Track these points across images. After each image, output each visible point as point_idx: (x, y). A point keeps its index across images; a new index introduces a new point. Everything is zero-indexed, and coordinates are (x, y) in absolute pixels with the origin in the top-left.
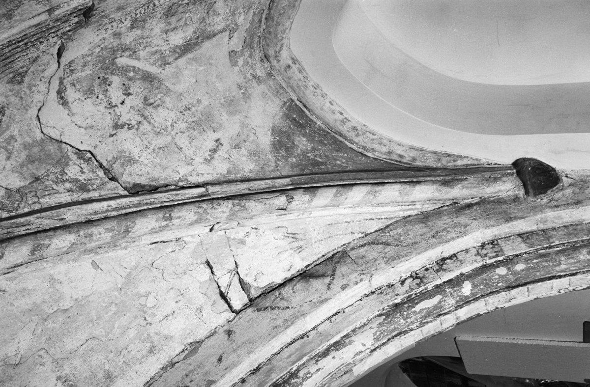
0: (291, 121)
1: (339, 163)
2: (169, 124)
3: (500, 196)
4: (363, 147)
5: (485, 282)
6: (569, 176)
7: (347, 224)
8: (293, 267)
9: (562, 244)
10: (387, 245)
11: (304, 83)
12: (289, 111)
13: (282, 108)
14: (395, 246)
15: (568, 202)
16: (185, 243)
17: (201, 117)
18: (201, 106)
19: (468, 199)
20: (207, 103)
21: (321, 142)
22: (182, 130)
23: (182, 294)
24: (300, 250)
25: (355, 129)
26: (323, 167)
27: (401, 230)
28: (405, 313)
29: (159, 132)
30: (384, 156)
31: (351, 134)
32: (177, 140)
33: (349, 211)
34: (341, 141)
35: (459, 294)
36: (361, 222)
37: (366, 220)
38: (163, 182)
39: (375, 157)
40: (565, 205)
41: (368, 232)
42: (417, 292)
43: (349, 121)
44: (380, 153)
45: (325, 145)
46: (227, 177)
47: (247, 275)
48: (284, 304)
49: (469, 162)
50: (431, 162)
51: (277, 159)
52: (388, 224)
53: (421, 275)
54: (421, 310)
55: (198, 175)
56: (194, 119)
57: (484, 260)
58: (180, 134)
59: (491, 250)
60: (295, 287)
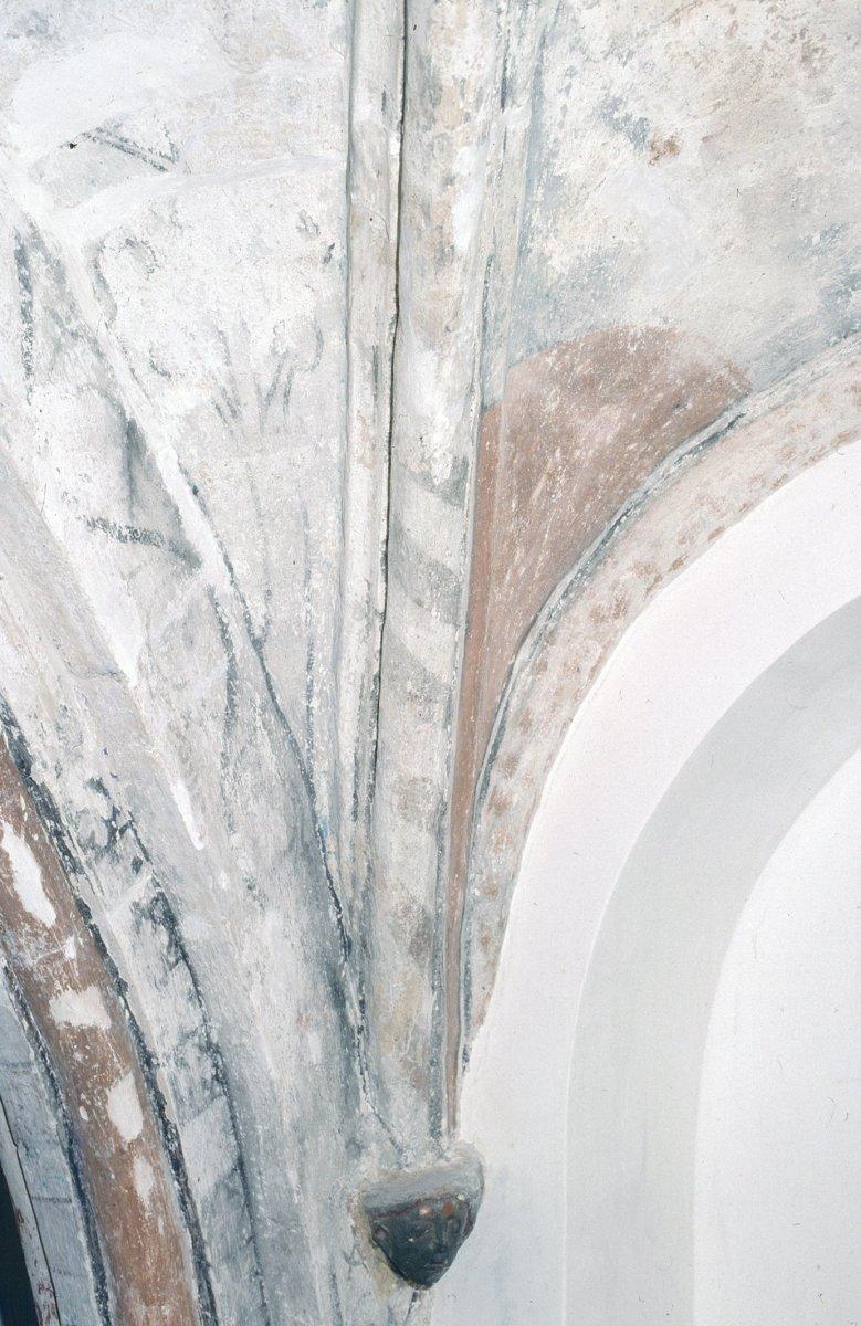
0: (678, 394)
1: (517, 558)
3: (362, 1094)
4: (552, 633)
5: (97, 1066)
6: (418, 1302)
9: (212, 1302)
10: (227, 726)
11: (801, 449)
13: (728, 365)
14: (223, 754)
15: (343, 1314)
19: (360, 990)
21: (591, 490)
22: (741, 27)
24: (227, 412)
25: (621, 609)
26: (514, 505)
27: (273, 769)
30: (514, 702)
31: (601, 593)
33: (356, 588)
34: (579, 557)
35: (57, 983)
37: (311, 646)
39: (515, 672)
40: (338, 1305)
42: (66, 839)
43: (649, 590)
44: (530, 689)
45: (579, 507)
48: (41, 360)
49: (475, 990)
50: (487, 862)
51: (565, 348)
52: (289, 717)
53: (119, 847)
55: (571, 72)
56: (766, 72)
57: (168, 1058)
58: (727, 22)
59: (197, 1079)
60: (95, 393)
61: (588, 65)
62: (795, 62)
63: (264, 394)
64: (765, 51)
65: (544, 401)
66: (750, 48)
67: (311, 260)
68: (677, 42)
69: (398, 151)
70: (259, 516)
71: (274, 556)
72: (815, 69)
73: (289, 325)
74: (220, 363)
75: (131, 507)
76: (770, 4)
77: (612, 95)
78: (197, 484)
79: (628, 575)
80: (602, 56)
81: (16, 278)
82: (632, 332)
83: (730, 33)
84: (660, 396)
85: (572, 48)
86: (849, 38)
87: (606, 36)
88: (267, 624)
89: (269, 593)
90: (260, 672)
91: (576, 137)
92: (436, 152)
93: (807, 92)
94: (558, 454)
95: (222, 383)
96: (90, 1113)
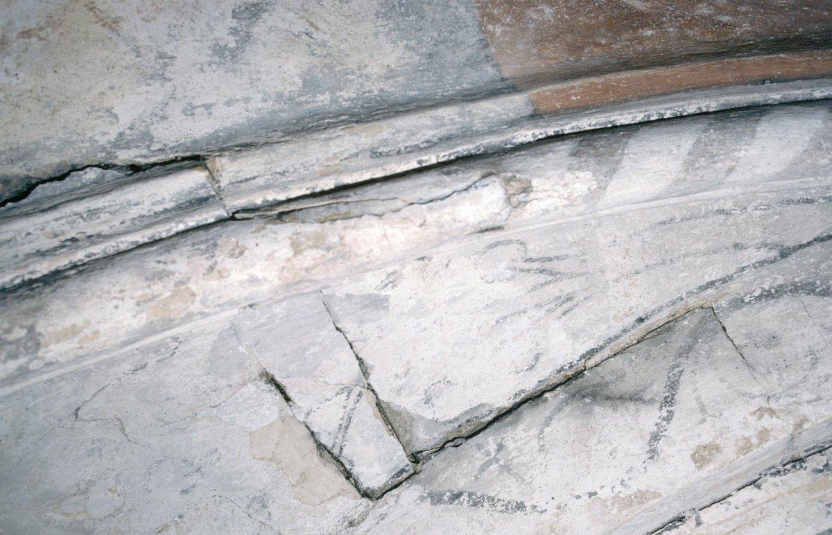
7: (723, 217)
8: (542, 359)
23: (198, 470)
26: (649, 33)
36: (770, 212)
37: (789, 202)
38: (56, 160)
41: (791, 244)
47: (399, 392)
48: (508, 490)
55: (190, 111)
60: (547, 430)
61: (179, 96)
63: (550, 278)
65: (544, 22)
68: (139, 12)
70: (664, 263)
71: (702, 246)
74: (524, 318)
75: (644, 402)
77: (209, 59)
78: (634, 318)
80: (168, 84)
81: (451, 506)
85: (164, 118)
87: (143, 88)
88: (766, 245)
89: (736, 246)
90: (811, 249)
91: (259, 79)
95: (542, 313)
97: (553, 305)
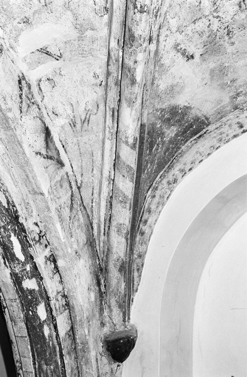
0: (191, 124)
1: (148, 166)
2: (220, 14)
3: (105, 310)
4: (157, 187)
5: (35, 300)
6: (119, 367)
8: (56, 116)
10: (71, 209)
11: (224, 139)
12: (200, 122)
13: (205, 116)
14: (70, 217)
15: (99, 369)
16: (102, 16)
17: (218, 44)
18: (227, 45)
19: (104, 282)
20: (228, 51)
21: (168, 149)
22: (212, 25)
23: (46, 5)
24: (72, 125)
25: (175, 181)
26: (148, 152)
27: (82, 221)
28: (9, 227)
29: (215, 4)
30: (146, 206)
31: (170, 177)
32: (204, 20)
33: (106, 174)
34: (164, 167)
35: (24, 277)
36: (91, 184)
37: (93, 189)
39: (147, 198)
40: (98, 367)
42: (28, 238)
43: (183, 176)
44: (150, 202)
45: (165, 154)
46: (158, 63)
48: (24, 109)
49: (135, 283)
50: (139, 248)
51: (162, 110)
52: (87, 208)
53: (42, 240)
54: (11, 242)
55: (167, 36)
56: (218, 37)
57: (53, 298)
58: (208, 23)
59: (61, 304)
60: (38, 119)
62: (225, 35)
63: (83, 121)
64: (218, 32)
65: (157, 124)
66: (214, 31)
67: (96, 85)
68: (195, 28)
69: (122, 55)
70: (80, 154)
71: (84, 165)
72: (230, 37)
73: (90, 102)
74: (71, 112)
75: (47, 150)
76: (219, 19)
78: (64, 145)
79: (178, 172)
80: (175, 32)
81: (18, 87)
82: (180, 106)
83: (209, 27)
84: (187, 124)
85: (167, 30)
86: (239, 29)
87: (176, 26)
88: (82, 183)
89: (82, 174)
90: (79, 195)
92: (133, 54)
93: (228, 43)
94: (160, 139)
95: (71, 117)
96: (32, 313)
97: (73, 121)
